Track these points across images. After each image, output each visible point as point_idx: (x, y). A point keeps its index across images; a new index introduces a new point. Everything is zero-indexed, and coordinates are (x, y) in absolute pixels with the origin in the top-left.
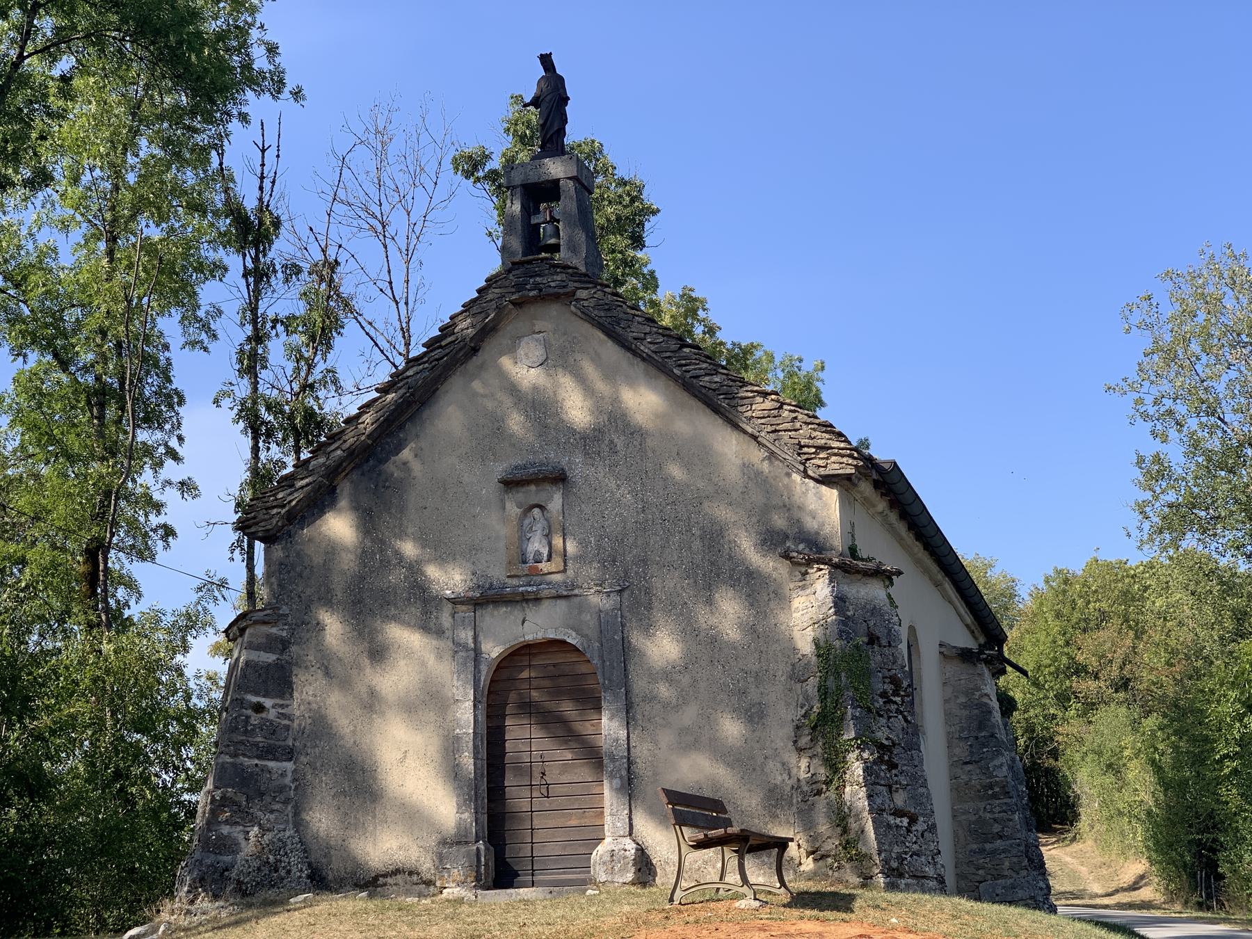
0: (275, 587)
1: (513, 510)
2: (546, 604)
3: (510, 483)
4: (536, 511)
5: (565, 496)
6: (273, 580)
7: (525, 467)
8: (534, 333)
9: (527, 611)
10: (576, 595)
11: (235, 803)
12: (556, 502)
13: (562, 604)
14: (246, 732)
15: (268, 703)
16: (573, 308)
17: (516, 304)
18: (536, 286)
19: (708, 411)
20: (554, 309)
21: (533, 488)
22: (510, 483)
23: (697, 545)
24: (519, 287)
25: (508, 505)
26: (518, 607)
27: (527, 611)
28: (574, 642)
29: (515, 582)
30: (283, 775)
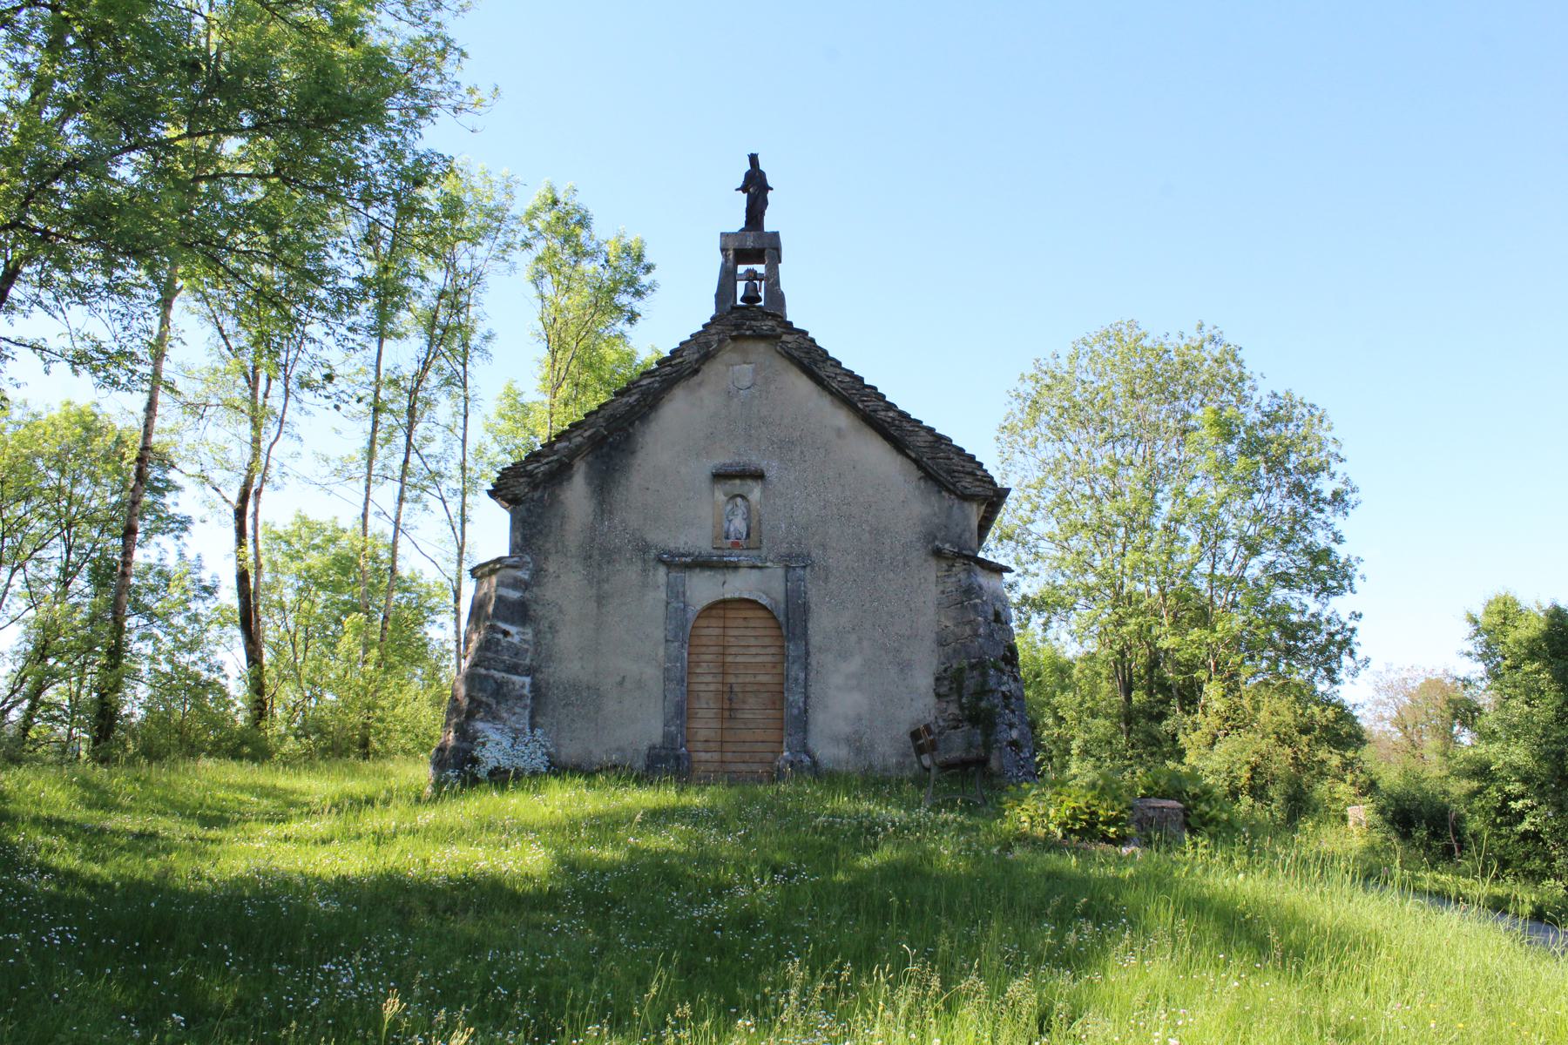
1: (720, 496)
2: (743, 571)
3: (720, 476)
4: (739, 500)
5: (763, 492)
11: (488, 705)
12: (755, 492)
14: (497, 652)
15: (512, 629)
17: (734, 339)
20: (762, 347)
21: (737, 482)
22: (720, 476)
24: (737, 327)
29: (719, 552)
30: (523, 687)
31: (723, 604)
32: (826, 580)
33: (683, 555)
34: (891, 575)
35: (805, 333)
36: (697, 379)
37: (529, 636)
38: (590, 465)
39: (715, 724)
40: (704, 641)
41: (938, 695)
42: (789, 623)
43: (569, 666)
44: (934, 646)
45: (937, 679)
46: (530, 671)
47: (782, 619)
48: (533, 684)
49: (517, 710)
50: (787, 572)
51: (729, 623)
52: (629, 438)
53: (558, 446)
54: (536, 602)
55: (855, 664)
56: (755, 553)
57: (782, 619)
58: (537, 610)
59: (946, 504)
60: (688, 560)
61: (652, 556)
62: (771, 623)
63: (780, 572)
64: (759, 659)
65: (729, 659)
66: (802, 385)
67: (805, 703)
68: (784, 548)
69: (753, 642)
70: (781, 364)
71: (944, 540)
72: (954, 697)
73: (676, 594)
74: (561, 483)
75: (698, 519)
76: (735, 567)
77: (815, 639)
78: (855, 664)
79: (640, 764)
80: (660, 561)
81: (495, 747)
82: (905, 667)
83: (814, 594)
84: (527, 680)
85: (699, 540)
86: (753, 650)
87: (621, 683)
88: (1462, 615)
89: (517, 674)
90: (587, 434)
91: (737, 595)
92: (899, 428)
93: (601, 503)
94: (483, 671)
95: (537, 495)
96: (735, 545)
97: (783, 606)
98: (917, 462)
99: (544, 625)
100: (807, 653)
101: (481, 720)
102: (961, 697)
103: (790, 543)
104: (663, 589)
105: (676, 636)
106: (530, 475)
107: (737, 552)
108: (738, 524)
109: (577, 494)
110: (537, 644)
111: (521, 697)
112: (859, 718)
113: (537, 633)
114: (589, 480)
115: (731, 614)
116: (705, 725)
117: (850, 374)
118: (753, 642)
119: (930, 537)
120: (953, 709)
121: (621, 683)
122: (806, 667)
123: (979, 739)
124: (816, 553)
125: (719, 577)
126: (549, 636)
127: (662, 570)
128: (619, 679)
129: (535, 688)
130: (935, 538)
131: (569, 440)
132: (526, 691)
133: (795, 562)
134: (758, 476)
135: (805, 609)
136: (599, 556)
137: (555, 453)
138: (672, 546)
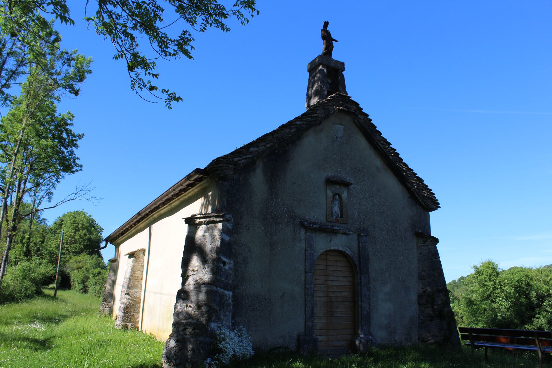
0: (225, 203)
1: (330, 194)
2: (339, 235)
3: (330, 182)
4: (337, 196)
5: (348, 192)
6: (224, 199)
10: (350, 234)
11: (217, 311)
16: (356, 120)
21: (338, 186)
22: (330, 182)
28: (349, 253)
29: (329, 224)
33: (313, 223)
37: (232, 266)
41: (419, 304)
42: (356, 266)
45: (419, 296)
46: (233, 288)
47: (357, 263)
49: (227, 313)
53: (251, 149)
60: (317, 226)
63: (356, 237)
64: (342, 284)
65: (330, 283)
66: (363, 143)
73: (309, 245)
75: (318, 206)
76: (335, 232)
79: (293, 346)
80: (302, 225)
84: (231, 293)
85: (318, 215)
89: (228, 290)
90: (268, 146)
91: (336, 248)
94: (215, 288)
96: (337, 221)
97: (357, 256)
101: (215, 321)
104: (303, 241)
106: (236, 164)
108: (336, 209)
109: (258, 180)
113: (236, 264)
116: (320, 322)
117: (385, 140)
120: (429, 311)
127: (303, 232)
131: (258, 147)
132: (230, 301)
134: (347, 185)
137: (251, 153)
138: (307, 217)
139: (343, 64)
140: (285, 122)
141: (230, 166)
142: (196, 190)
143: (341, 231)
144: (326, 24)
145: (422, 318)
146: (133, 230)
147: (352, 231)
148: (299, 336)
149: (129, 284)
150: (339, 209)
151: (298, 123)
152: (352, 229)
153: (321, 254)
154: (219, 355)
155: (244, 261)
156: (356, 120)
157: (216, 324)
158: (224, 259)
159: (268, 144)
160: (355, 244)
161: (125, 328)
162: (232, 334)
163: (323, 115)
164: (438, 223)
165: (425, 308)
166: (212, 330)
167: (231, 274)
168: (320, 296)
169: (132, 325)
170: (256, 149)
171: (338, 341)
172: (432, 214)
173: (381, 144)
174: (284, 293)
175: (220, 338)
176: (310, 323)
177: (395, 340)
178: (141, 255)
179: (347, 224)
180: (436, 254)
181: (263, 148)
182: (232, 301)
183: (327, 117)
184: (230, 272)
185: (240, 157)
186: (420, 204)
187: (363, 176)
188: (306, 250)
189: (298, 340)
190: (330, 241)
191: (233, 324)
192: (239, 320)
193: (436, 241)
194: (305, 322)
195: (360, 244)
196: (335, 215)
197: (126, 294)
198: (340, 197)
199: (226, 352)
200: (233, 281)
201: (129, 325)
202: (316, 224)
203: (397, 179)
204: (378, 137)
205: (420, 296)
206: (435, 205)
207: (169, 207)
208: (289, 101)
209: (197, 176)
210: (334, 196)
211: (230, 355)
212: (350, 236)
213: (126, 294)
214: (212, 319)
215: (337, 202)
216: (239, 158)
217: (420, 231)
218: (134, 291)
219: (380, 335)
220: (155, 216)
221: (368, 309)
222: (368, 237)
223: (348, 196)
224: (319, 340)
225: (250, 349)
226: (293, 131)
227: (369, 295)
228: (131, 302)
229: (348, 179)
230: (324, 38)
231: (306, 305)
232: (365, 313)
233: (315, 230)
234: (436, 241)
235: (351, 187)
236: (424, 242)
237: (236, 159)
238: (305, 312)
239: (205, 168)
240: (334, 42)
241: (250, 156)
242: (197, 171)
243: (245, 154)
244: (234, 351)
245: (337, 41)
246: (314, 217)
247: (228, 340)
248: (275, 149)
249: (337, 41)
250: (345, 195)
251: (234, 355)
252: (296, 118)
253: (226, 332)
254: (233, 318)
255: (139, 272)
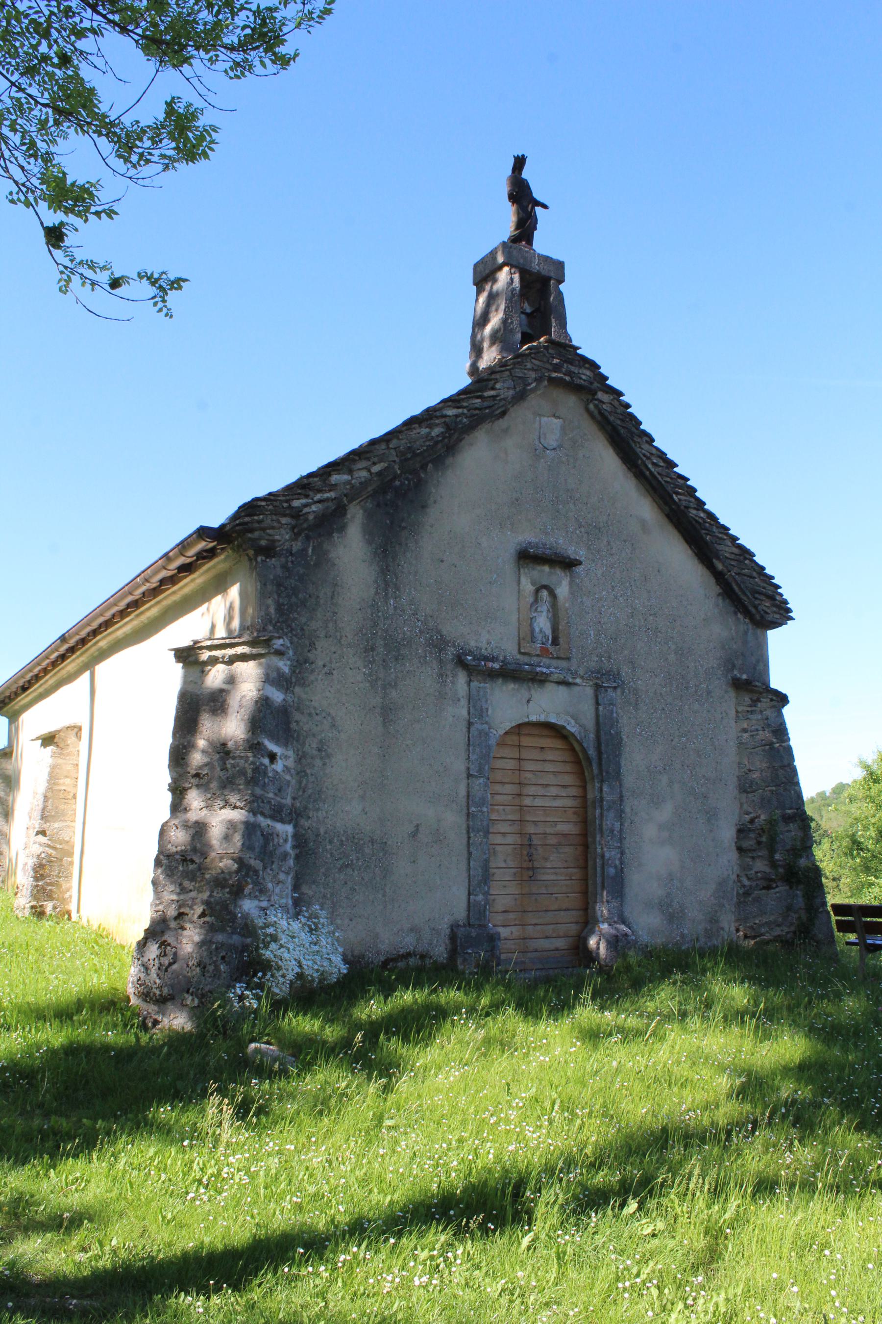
0: (272, 610)
1: (528, 587)
2: (550, 687)
3: (527, 557)
4: (545, 593)
5: (571, 584)
6: (270, 601)
7: (536, 546)
8: (554, 416)
9: (533, 692)
10: (576, 684)
11: (256, 872)
13: (562, 689)
14: (264, 786)
16: (591, 406)
18: (569, 373)
19: (682, 540)
21: (546, 568)
22: (527, 557)
23: (672, 657)
25: (524, 580)
26: (525, 686)
27: (533, 692)
28: (573, 730)
29: (526, 659)
31: (520, 729)
32: (636, 706)
33: (486, 659)
34: (696, 706)
35: (620, 394)
36: (503, 423)
37: (290, 763)
38: (369, 515)
39: (513, 889)
40: (498, 776)
41: (740, 849)
42: (591, 760)
43: (346, 811)
44: (736, 792)
45: (740, 831)
46: (294, 816)
47: (592, 752)
48: (296, 836)
49: (282, 876)
50: (596, 691)
51: (525, 754)
52: (419, 485)
53: (335, 478)
54: (298, 709)
55: (666, 813)
56: (563, 664)
57: (592, 752)
58: (301, 722)
59: (742, 627)
60: (496, 666)
61: (450, 657)
62: (567, 756)
63: (589, 691)
64: (559, 803)
65: (527, 801)
66: (607, 460)
67: (621, 859)
68: (593, 663)
69: (550, 779)
70: (590, 428)
71: (741, 671)
72: (764, 852)
73: (477, 711)
74: (330, 534)
75: (501, 616)
76: (538, 680)
77: (629, 780)
78: (666, 813)
79: (440, 951)
80: (460, 662)
81: (300, 947)
82: (711, 815)
83: (627, 723)
84: (289, 829)
85: (499, 639)
86: (554, 791)
87: (414, 835)
88: (856, 760)
89: (282, 821)
90: (376, 469)
91: (543, 718)
92: (710, 532)
93: (384, 571)
95: (297, 546)
96: (544, 652)
97: (592, 736)
98: (719, 577)
99: (310, 747)
100: (621, 798)
101: (251, 896)
102: (772, 851)
103: (600, 656)
104: (464, 702)
105: (480, 770)
106: (296, 514)
107: (545, 661)
108: (543, 623)
109: (351, 552)
110: (301, 774)
111: (285, 856)
112: (671, 877)
113: (301, 758)
114: (369, 533)
115: (526, 741)
117: (662, 455)
118: (550, 779)
119: (729, 664)
120: (761, 866)
121: (414, 835)
122: (620, 815)
123: (800, 902)
124: (625, 670)
125: (524, 693)
126: (318, 762)
127: (462, 678)
128: (411, 829)
129: (300, 840)
130: (734, 666)
131: (350, 472)
132: (288, 847)
133: (604, 681)
135: (617, 744)
136: (384, 648)
137: (333, 487)
138: (473, 644)
139: (560, 265)
140: (417, 410)
141: (284, 520)
142: (200, 581)
143: (555, 677)
144: (520, 163)
145: (746, 882)
146: (50, 680)
147: (582, 677)
148: (454, 927)
149: (44, 809)
150: (548, 625)
151: (450, 412)
152: (581, 672)
153: (506, 733)
154: (264, 975)
155: (319, 750)
156: (591, 406)
157: (256, 902)
158: (272, 746)
159: (374, 464)
160: (587, 709)
161: (39, 913)
162: (295, 926)
163: (511, 392)
164: (786, 656)
165: (753, 858)
166: (246, 916)
167: (289, 782)
168: (504, 834)
169: (55, 908)
170: (346, 477)
171: (547, 937)
172: (772, 634)
173: (654, 464)
174: (417, 826)
175: (266, 935)
176: (480, 897)
177: (683, 936)
178: (72, 739)
179: (568, 659)
180: (781, 731)
181: (364, 474)
182: (294, 847)
183: (521, 396)
184: (288, 777)
185: (307, 496)
186: (747, 613)
187: (609, 543)
188: (470, 724)
189: (453, 937)
190: (528, 701)
191: (297, 903)
192: (311, 893)
193: (782, 699)
194: (469, 894)
195: (601, 708)
196: (539, 637)
197: (38, 833)
198: (553, 594)
199: (279, 968)
200: (294, 799)
201: (49, 907)
202: (493, 659)
203: (690, 552)
204: (646, 447)
205: (741, 831)
206: (780, 613)
207: (135, 623)
208: (426, 357)
209: (202, 545)
210: (537, 591)
211: (290, 976)
212: (576, 689)
213: (38, 833)
214: (246, 891)
215: (544, 608)
216: (304, 501)
217: (744, 677)
218: (56, 825)
219: (647, 925)
220: (103, 644)
221: (617, 862)
222: (619, 691)
223: (572, 592)
224: (502, 936)
225: (337, 959)
226: (436, 431)
227: (621, 830)
228: (50, 851)
229: (572, 551)
230: (514, 198)
231: (470, 854)
232: (612, 871)
233: (492, 675)
234: (782, 699)
235: (579, 569)
236: (755, 702)
237: (296, 503)
238: (469, 869)
239: (223, 526)
240: (538, 209)
241: (332, 495)
242: (203, 532)
243: (320, 491)
244: (300, 966)
245: (545, 207)
246: (489, 643)
247: (284, 939)
248: (393, 477)
249: (545, 207)
250: (563, 590)
251: (300, 976)
252: (444, 401)
253: (282, 922)
254: (296, 887)
255: (68, 781)
